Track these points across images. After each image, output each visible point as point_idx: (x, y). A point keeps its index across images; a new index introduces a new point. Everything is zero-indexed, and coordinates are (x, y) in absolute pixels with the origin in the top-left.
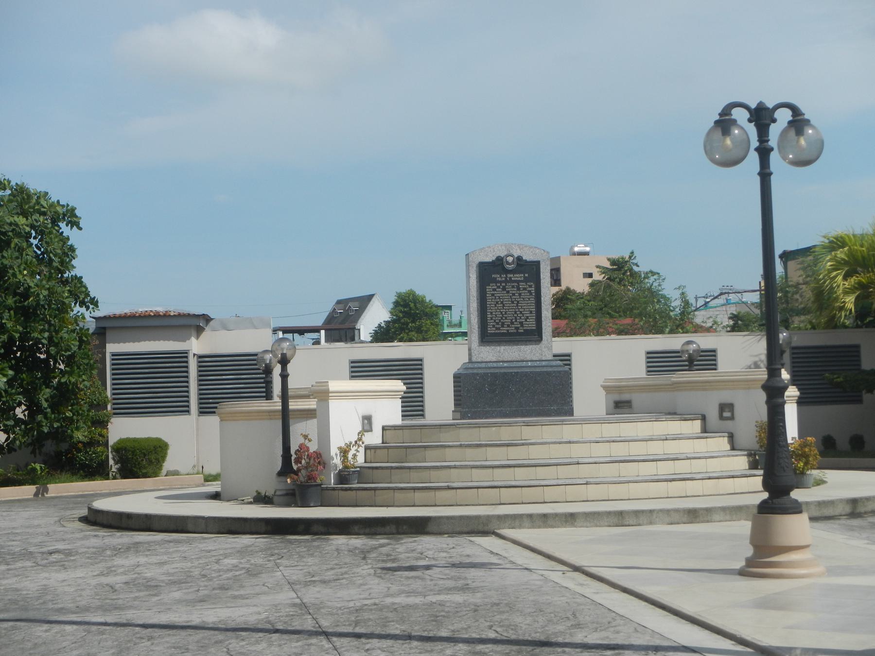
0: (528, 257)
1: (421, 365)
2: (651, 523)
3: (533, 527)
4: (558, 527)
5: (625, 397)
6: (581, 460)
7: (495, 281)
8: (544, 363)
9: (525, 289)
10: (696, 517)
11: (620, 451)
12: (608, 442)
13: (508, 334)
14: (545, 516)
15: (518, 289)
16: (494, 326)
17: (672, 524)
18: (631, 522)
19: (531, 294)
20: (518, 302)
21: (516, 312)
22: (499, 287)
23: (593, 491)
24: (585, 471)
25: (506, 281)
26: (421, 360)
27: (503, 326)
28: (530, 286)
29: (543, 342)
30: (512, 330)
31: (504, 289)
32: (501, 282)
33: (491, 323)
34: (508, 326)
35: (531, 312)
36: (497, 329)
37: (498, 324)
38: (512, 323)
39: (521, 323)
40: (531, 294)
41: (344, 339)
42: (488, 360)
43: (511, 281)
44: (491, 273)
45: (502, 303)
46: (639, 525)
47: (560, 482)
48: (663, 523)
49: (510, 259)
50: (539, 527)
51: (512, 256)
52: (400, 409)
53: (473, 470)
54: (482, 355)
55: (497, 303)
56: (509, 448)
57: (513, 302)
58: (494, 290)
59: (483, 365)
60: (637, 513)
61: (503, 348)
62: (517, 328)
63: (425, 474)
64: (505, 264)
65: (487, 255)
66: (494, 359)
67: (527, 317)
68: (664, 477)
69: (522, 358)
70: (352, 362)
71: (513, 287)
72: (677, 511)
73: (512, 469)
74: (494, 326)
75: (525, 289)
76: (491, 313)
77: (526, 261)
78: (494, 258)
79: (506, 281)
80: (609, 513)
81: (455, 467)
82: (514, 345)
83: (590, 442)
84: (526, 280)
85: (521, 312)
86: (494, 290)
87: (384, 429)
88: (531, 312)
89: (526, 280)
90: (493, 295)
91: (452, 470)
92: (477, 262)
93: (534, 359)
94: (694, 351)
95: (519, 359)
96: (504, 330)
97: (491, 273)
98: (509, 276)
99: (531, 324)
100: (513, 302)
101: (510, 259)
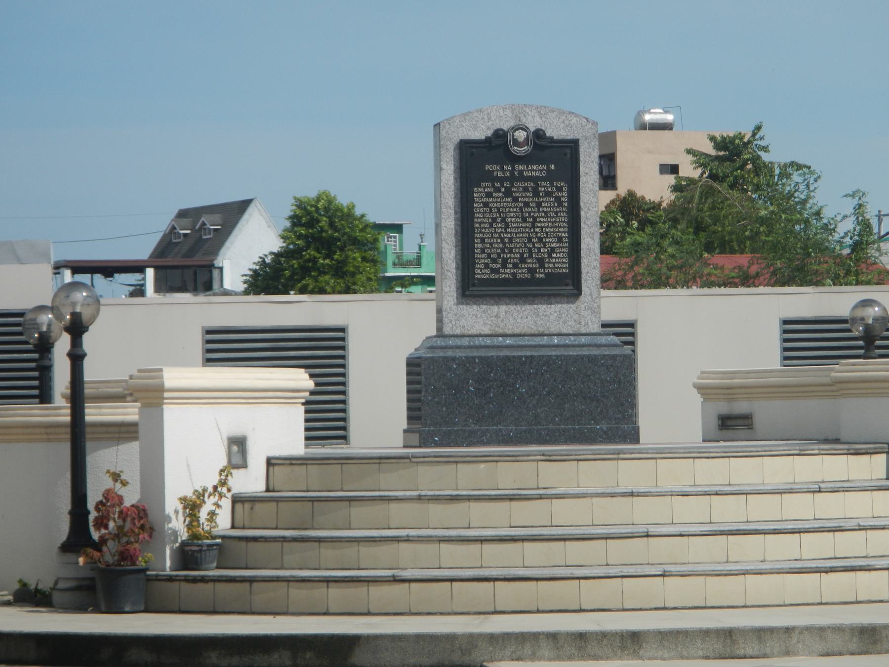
0: (556, 131)
1: (343, 339)
2: (787, 653)
3: (558, 658)
4: (608, 658)
5: (741, 407)
6: (653, 530)
7: (490, 177)
8: (583, 340)
9: (548, 194)
10: (875, 643)
11: (728, 511)
12: (706, 494)
13: (515, 281)
14: (581, 637)
15: (536, 194)
16: (487, 266)
17: (828, 655)
18: (749, 651)
19: (560, 204)
20: (535, 219)
21: (530, 240)
22: (497, 190)
23: (675, 590)
24: (660, 551)
25: (512, 179)
26: (343, 330)
27: (504, 266)
28: (560, 189)
29: (582, 298)
30: (523, 273)
31: (508, 193)
32: (502, 180)
33: (481, 260)
34: (515, 266)
35: (560, 240)
36: (495, 271)
37: (494, 261)
38: (523, 260)
39: (541, 261)
40: (560, 204)
42: (474, 331)
43: (522, 178)
44: (483, 162)
45: (504, 220)
46: (765, 656)
47: (612, 571)
48: (810, 654)
49: (521, 135)
50: (570, 658)
51: (525, 129)
52: (302, 425)
53: (444, 546)
54: (463, 322)
55: (494, 220)
56: (513, 503)
58: (489, 195)
59: (465, 342)
60: (761, 633)
61: (503, 308)
62: (532, 271)
63: (349, 552)
65: (475, 127)
66: (486, 330)
67: (553, 250)
68: (813, 564)
69: (541, 329)
70: (209, 332)
71: (526, 189)
72: (838, 629)
73: (519, 545)
74: (487, 266)
76: (483, 241)
77: (551, 138)
78: (489, 133)
79: (512, 179)
80: (706, 633)
81: (408, 539)
82: (525, 303)
83: (672, 494)
84: (551, 177)
86: (489, 195)
87: (270, 463)
88: (560, 240)
89: (551, 177)
90: (486, 205)
91: (403, 546)
92: (456, 140)
93: (564, 331)
94: (875, 319)
95: (534, 330)
96: (506, 274)
97: (483, 162)
98: (518, 167)
99: (559, 263)
100: (524, 220)
101: (521, 135)
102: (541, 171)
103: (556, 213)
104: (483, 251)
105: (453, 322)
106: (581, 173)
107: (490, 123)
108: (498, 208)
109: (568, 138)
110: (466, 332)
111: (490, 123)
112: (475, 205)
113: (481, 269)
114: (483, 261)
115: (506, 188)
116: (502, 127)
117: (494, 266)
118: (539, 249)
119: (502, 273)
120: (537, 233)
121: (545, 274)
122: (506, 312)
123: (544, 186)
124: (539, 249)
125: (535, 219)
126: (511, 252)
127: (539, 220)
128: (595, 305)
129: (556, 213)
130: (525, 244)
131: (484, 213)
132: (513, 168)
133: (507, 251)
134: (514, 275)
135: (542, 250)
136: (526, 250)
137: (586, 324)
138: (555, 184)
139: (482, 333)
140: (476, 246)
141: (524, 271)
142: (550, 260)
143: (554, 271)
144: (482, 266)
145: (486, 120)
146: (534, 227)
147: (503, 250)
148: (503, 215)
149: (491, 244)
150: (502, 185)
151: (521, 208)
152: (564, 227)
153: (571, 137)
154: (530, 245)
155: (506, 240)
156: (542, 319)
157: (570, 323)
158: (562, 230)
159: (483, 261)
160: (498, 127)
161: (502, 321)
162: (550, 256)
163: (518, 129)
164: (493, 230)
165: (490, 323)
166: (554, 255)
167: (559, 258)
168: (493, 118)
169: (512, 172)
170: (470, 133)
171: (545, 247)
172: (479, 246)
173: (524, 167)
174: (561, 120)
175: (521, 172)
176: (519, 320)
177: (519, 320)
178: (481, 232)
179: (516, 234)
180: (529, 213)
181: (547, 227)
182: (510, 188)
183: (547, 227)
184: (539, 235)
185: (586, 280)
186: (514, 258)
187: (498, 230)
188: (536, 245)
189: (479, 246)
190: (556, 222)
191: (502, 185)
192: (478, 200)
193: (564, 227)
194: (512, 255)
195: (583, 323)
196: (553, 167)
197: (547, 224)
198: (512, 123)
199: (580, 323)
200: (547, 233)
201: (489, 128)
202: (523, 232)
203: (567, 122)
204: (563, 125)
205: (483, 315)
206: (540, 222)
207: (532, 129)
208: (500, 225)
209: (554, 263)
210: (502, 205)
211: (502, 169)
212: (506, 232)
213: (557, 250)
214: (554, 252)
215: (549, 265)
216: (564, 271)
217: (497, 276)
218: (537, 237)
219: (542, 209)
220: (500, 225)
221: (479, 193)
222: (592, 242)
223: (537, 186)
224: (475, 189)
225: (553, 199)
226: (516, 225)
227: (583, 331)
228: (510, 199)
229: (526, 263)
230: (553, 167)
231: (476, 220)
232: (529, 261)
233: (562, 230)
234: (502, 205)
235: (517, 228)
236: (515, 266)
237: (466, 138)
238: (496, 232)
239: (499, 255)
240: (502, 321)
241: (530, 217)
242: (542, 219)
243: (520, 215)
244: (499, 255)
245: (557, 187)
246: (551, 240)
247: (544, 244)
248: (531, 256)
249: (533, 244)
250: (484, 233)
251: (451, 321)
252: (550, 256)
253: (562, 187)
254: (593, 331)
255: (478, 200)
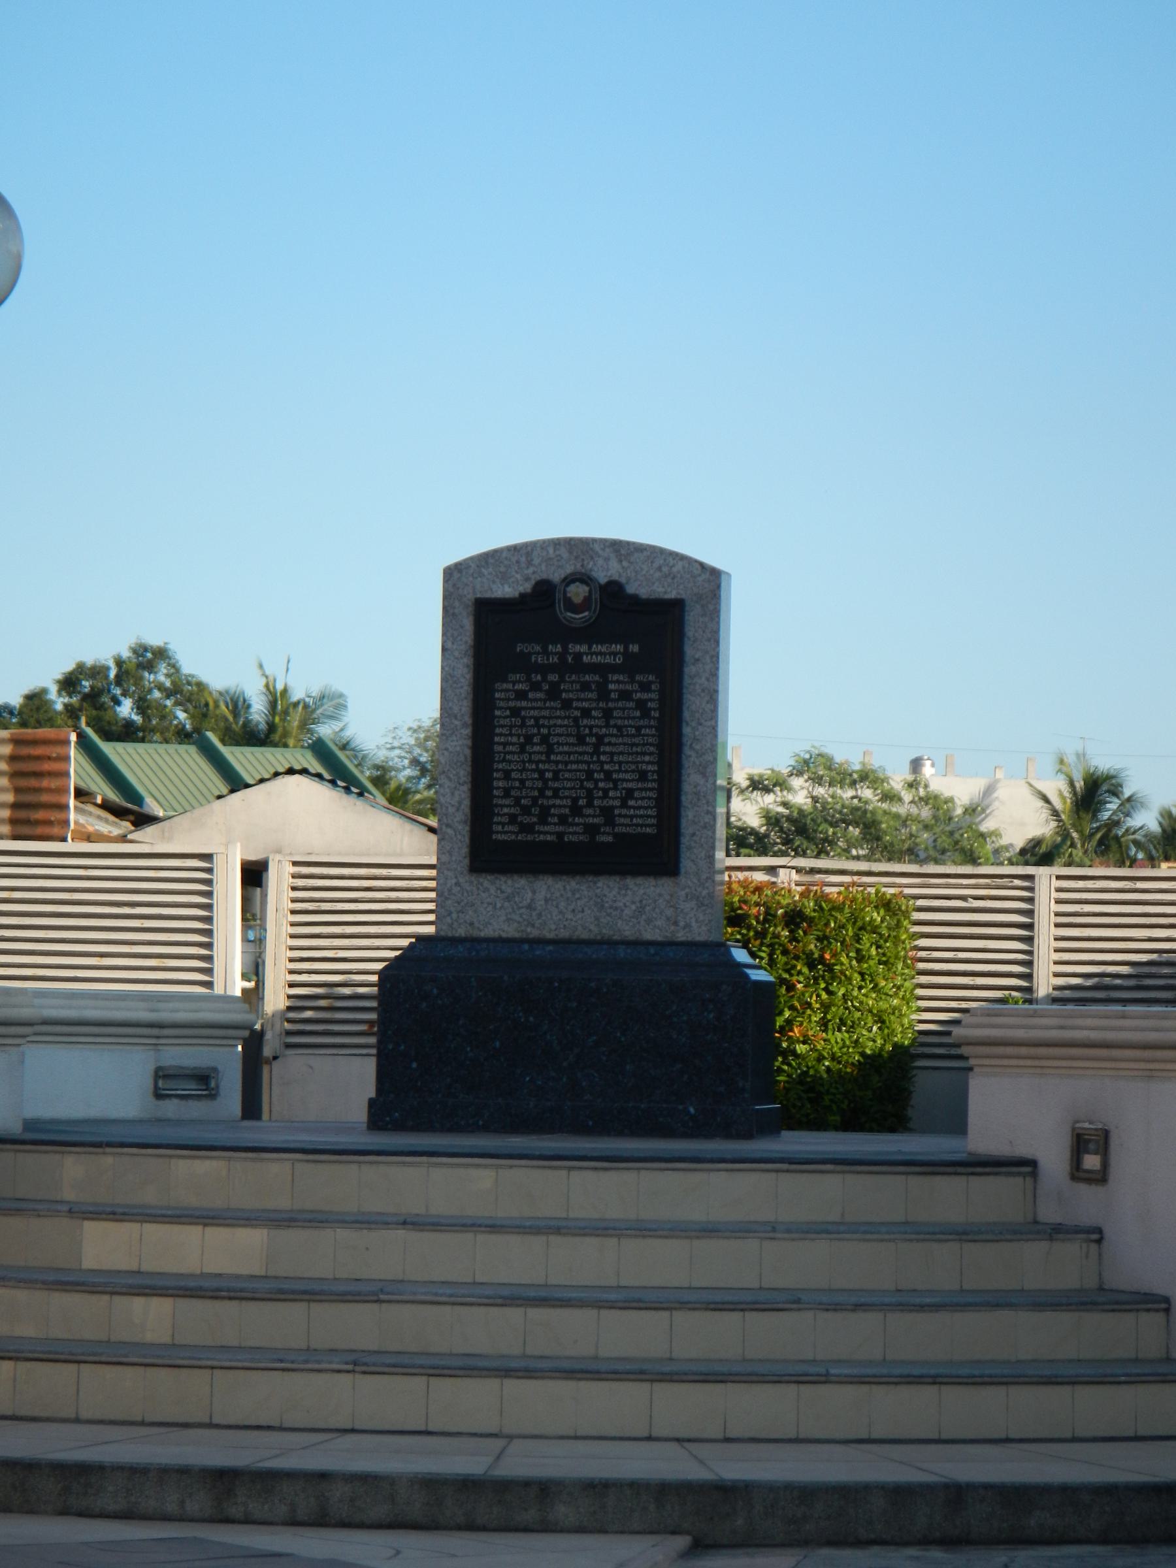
9: (625, 695)
15: (604, 695)
19: (646, 713)
20: (600, 739)
21: (589, 774)
22: (536, 687)
25: (563, 668)
27: (543, 820)
28: (645, 687)
30: (575, 834)
31: (554, 693)
32: (545, 669)
33: (505, 808)
34: (563, 820)
36: (527, 828)
37: (526, 810)
40: (646, 713)
41: (713, 723)
43: (578, 666)
45: (545, 739)
49: (578, 592)
55: (529, 739)
57: (581, 740)
58: (521, 695)
62: (592, 830)
64: (560, 608)
65: (504, 578)
67: (630, 793)
75: (625, 695)
76: (507, 775)
77: (635, 599)
78: (527, 587)
79: (563, 668)
84: (631, 666)
85: (608, 775)
86: (521, 695)
88: (643, 776)
89: (631, 666)
90: (515, 712)
96: (547, 833)
99: (640, 818)
100: (581, 740)
101: (578, 592)
102: (615, 654)
103: (638, 729)
104: (507, 793)
105: (454, 916)
106: (688, 658)
107: (531, 570)
108: (537, 719)
109: (667, 597)
110: (476, 933)
111: (531, 570)
112: (497, 713)
113: (503, 824)
114: (506, 810)
115: (552, 684)
116: (551, 577)
117: (526, 820)
118: (606, 791)
119: (540, 833)
120: (602, 763)
121: (615, 835)
122: (546, 900)
123: (618, 682)
124: (606, 791)
125: (600, 739)
126: (556, 795)
127: (606, 740)
128: (705, 892)
129: (638, 729)
130: (582, 781)
131: (511, 727)
132: (565, 648)
133: (549, 793)
134: (560, 835)
135: (611, 794)
136: (583, 793)
137: (687, 926)
138: (638, 678)
139: (504, 935)
140: (495, 783)
141: (579, 829)
142: (624, 811)
143: (629, 830)
144: (505, 819)
145: (523, 565)
146: (597, 752)
147: (541, 791)
148: (544, 731)
149: (522, 782)
150: (544, 679)
151: (576, 719)
152: (651, 754)
153: (673, 595)
154: (590, 785)
155: (549, 775)
156: (609, 915)
157: (659, 923)
158: (647, 758)
159: (506, 810)
160: (544, 576)
161: (540, 915)
162: (624, 805)
163: (573, 581)
164: (526, 757)
165: (517, 918)
166: (631, 803)
167: (639, 808)
168: (536, 561)
169: (562, 656)
170: (494, 587)
171: (615, 788)
172: (501, 784)
173: (584, 648)
174: (656, 565)
175: (578, 656)
176: (570, 916)
177: (570, 916)
178: (504, 760)
179: (566, 763)
180: (591, 728)
181: (621, 753)
182: (558, 684)
183: (621, 753)
184: (606, 767)
185: (689, 848)
186: (560, 806)
187: (535, 757)
188: (601, 785)
189: (501, 784)
190: (637, 745)
191: (544, 679)
192: (502, 704)
193: (651, 754)
194: (558, 802)
195: (682, 924)
196: (634, 648)
197: (621, 748)
198: (569, 569)
199: (676, 923)
200: (620, 763)
201: (527, 579)
202: (577, 762)
203: (665, 569)
204: (658, 575)
205: (506, 904)
206: (610, 744)
207: (603, 580)
208: (537, 748)
209: (632, 817)
210: (544, 713)
211: (545, 652)
212: (549, 761)
213: (636, 794)
214: (632, 798)
215: (622, 820)
216: (648, 830)
217: (530, 838)
218: (602, 770)
219: (612, 722)
220: (537, 748)
221: (502, 692)
222: (702, 782)
223: (606, 682)
224: (497, 685)
225: (632, 704)
226: (566, 749)
227: (681, 936)
228: (557, 704)
229: (581, 815)
230: (634, 648)
231: (496, 739)
232: (589, 811)
233: (647, 758)
234: (544, 713)
235: (569, 753)
236: (563, 820)
237: (488, 595)
238: (530, 761)
239: (535, 800)
240: (540, 915)
241: (591, 735)
242: (613, 740)
243: (574, 731)
244: (535, 800)
245: (641, 684)
246: (628, 776)
247: (615, 782)
248: (590, 804)
249: (596, 781)
250: (510, 762)
251: (450, 914)
252: (624, 805)
253: (651, 682)
254: (698, 939)
255: (502, 704)
